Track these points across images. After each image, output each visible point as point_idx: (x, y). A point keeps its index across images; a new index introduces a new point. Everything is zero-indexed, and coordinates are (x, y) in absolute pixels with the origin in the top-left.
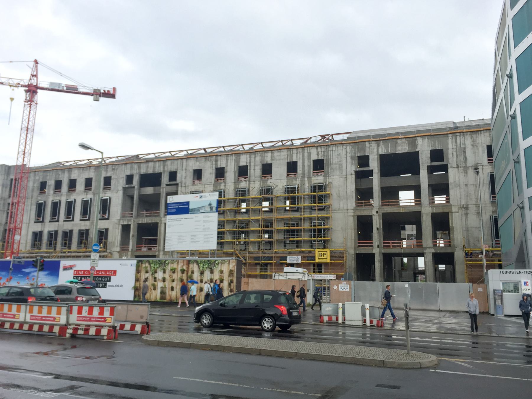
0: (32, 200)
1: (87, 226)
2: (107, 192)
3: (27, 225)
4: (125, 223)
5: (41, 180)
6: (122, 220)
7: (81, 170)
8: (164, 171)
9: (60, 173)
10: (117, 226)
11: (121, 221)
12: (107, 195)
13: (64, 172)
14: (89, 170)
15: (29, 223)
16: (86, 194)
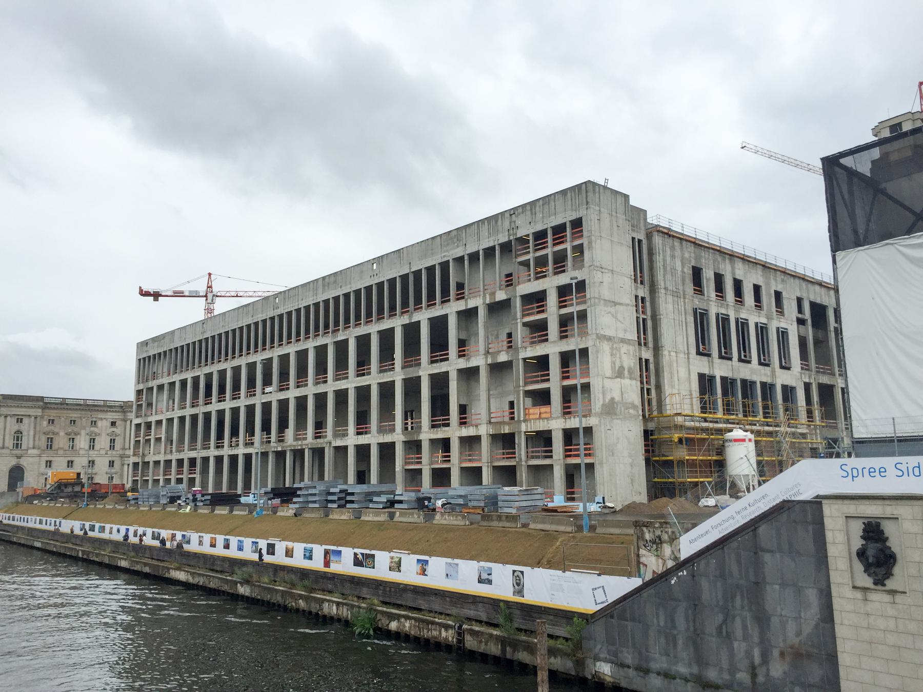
0: (685, 303)
1: (768, 376)
2: (781, 320)
3: (686, 357)
4: (807, 380)
5: (693, 264)
6: (804, 374)
7: (747, 266)
8: (829, 304)
9: (719, 259)
10: (800, 383)
11: (803, 376)
12: (783, 325)
13: (724, 259)
14: (757, 270)
15: (688, 353)
16: (757, 314)
